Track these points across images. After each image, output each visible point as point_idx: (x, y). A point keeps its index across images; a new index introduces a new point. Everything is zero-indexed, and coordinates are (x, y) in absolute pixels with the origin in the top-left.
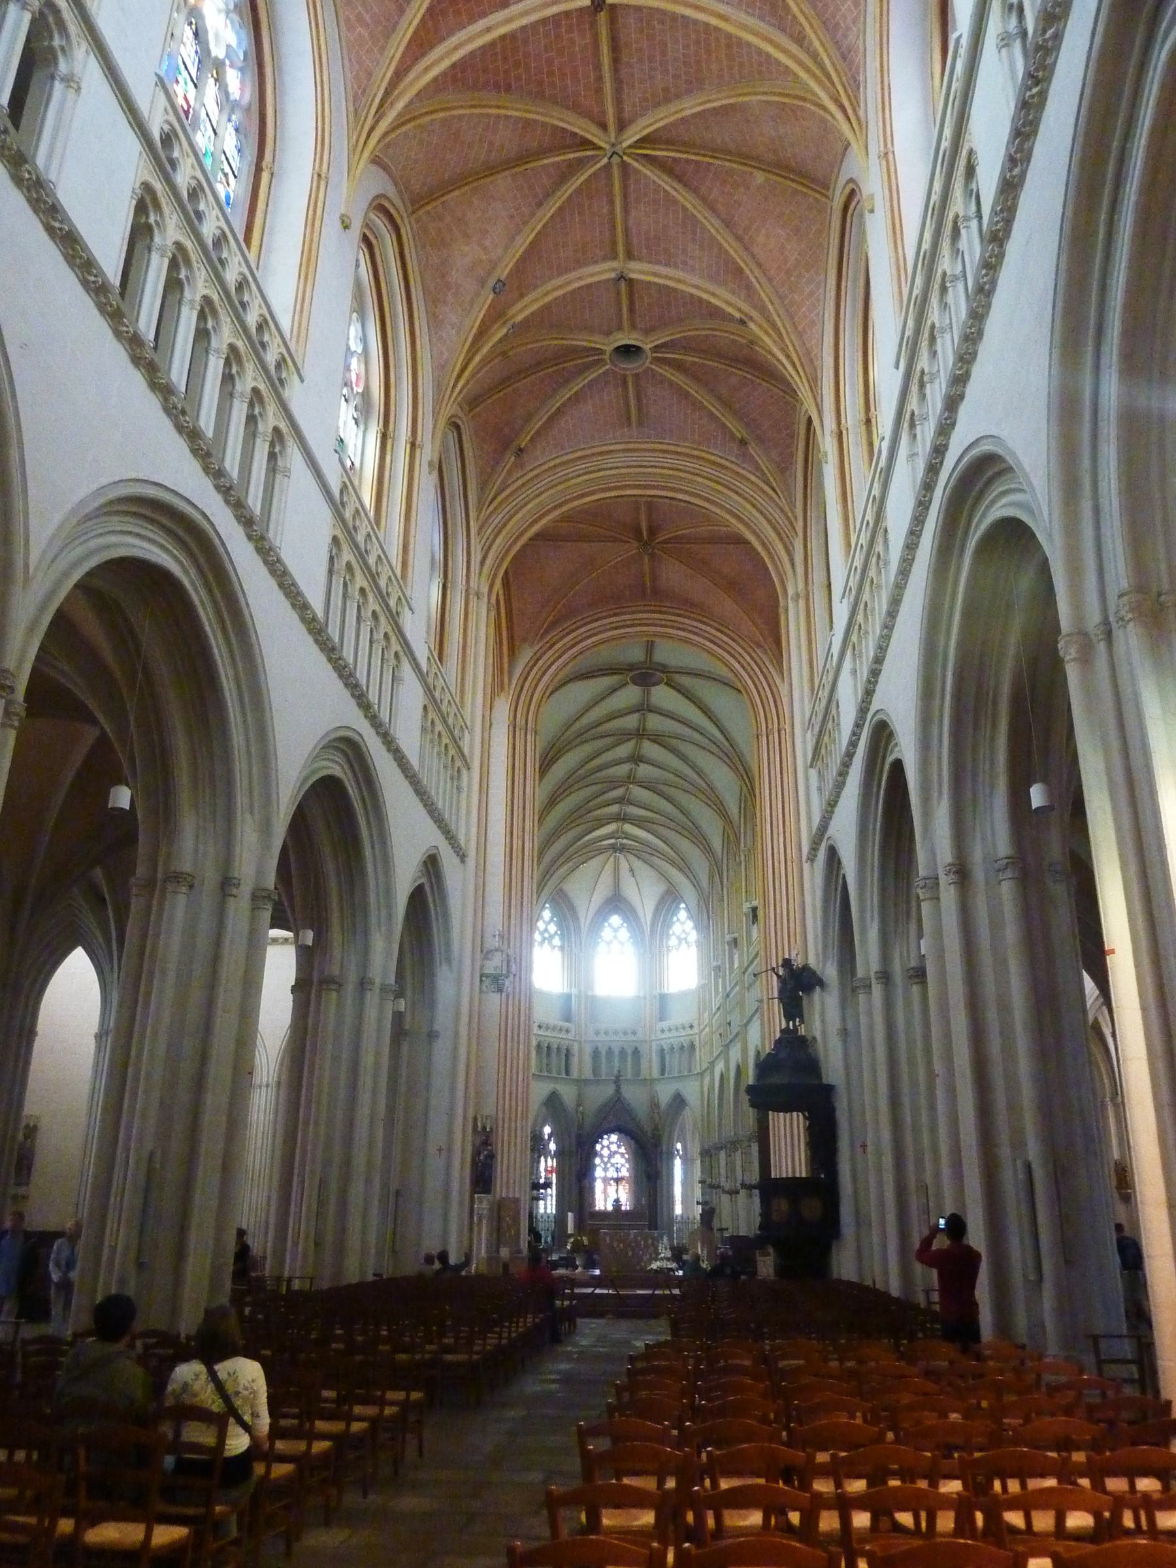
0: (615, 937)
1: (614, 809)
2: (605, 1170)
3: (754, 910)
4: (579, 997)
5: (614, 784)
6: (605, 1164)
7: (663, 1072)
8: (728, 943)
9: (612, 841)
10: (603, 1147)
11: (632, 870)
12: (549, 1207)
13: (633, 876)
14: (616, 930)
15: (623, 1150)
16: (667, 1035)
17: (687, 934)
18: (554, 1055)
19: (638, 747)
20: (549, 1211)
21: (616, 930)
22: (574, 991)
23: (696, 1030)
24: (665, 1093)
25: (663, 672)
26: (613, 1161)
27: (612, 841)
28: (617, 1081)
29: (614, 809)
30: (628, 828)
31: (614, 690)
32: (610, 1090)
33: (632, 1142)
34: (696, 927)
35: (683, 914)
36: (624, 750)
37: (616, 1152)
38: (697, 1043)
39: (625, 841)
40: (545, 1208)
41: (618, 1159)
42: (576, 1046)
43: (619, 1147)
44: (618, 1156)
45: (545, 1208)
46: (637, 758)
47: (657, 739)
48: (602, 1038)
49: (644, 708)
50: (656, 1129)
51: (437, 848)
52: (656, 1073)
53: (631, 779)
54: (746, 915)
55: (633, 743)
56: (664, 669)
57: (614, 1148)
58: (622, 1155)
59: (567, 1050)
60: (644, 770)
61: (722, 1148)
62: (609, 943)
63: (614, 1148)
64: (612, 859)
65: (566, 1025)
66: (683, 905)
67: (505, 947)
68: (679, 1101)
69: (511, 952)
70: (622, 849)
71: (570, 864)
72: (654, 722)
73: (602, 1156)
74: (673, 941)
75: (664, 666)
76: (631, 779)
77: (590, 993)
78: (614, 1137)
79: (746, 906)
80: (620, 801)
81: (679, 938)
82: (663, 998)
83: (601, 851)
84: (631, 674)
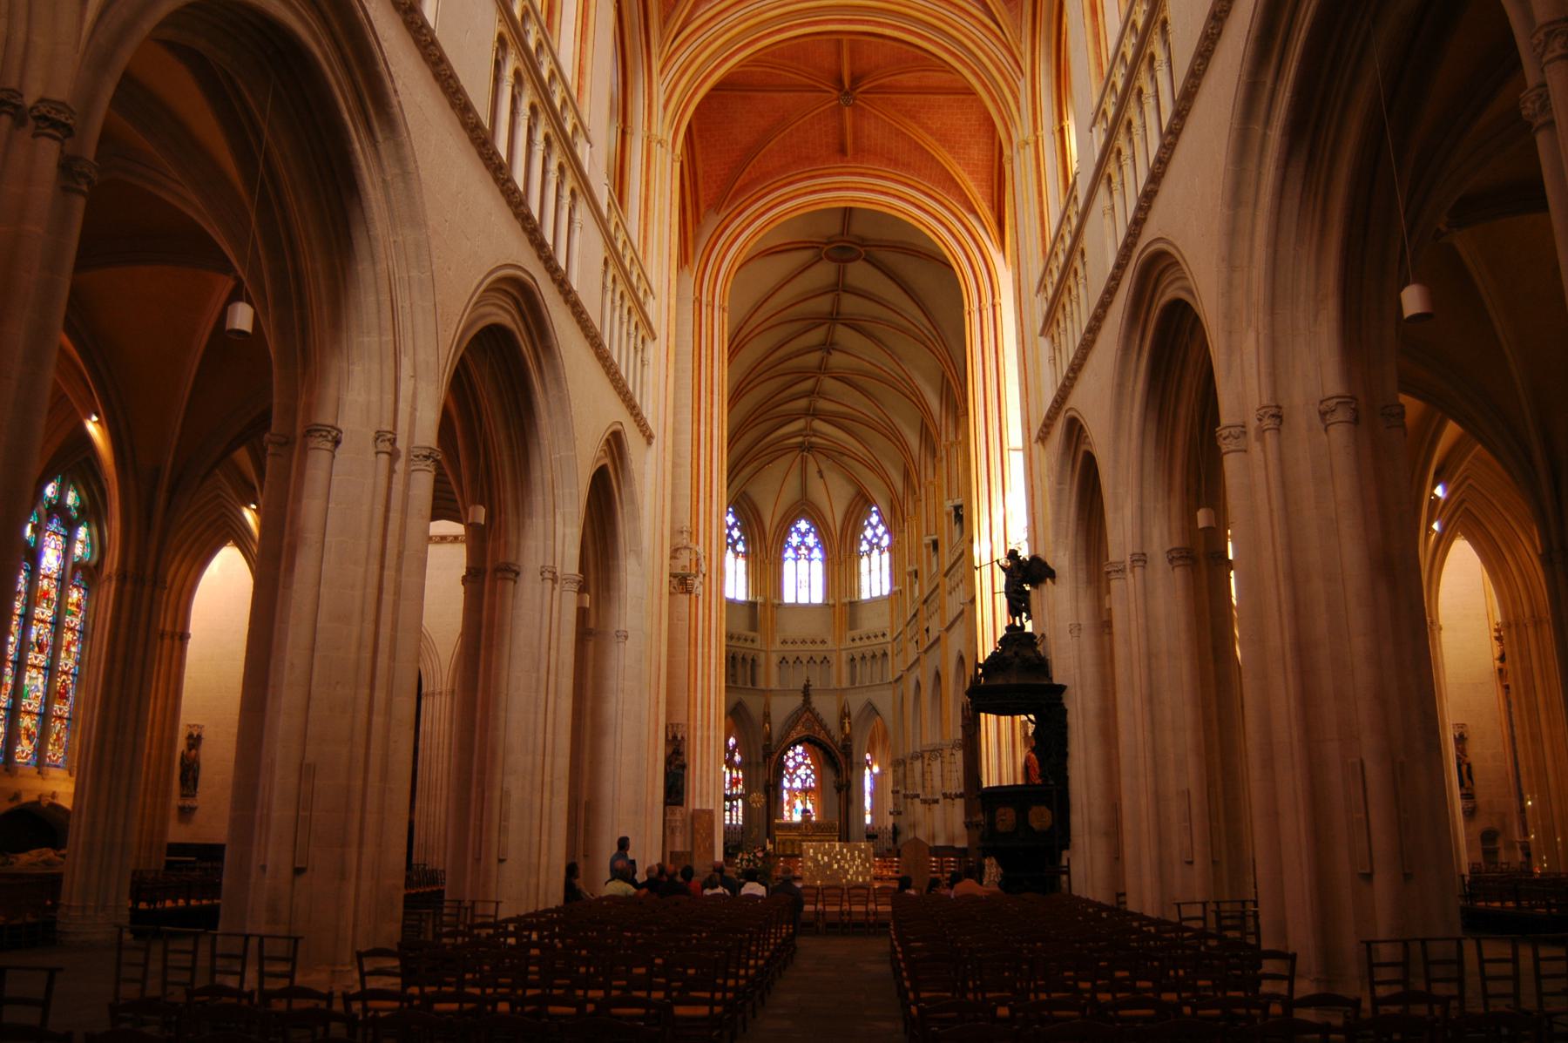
0: (803, 543)
1: (803, 403)
2: (791, 781)
3: (957, 508)
4: (764, 605)
5: (803, 373)
6: (791, 775)
7: (853, 681)
8: (927, 546)
9: (800, 439)
10: (788, 758)
11: (820, 472)
12: (734, 818)
13: (822, 477)
14: (803, 535)
15: (808, 761)
16: (858, 643)
17: (881, 539)
18: (739, 666)
19: (830, 332)
20: (734, 822)
21: (803, 535)
22: (760, 600)
23: (888, 638)
24: (856, 703)
25: (862, 246)
26: (799, 772)
27: (800, 439)
28: (806, 691)
29: (803, 403)
30: (818, 424)
31: (807, 267)
32: (798, 700)
33: (820, 753)
34: (888, 531)
35: (874, 519)
36: (816, 336)
37: (801, 764)
38: (890, 653)
39: (814, 439)
40: (731, 819)
41: (802, 771)
42: (762, 655)
43: (805, 758)
44: (803, 767)
45: (731, 819)
46: (828, 346)
47: (854, 325)
48: (790, 647)
49: (839, 287)
50: (848, 738)
51: (621, 424)
52: (845, 684)
53: (822, 368)
54: (948, 514)
55: (826, 326)
56: (863, 242)
57: (799, 759)
58: (808, 766)
59: (753, 660)
60: (837, 359)
61: (917, 758)
62: (796, 549)
63: (799, 759)
64: (799, 457)
65: (752, 634)
66: (874, 509)
67: (693, 545)
68: (871, 710)
69: (700, 549)
70: (811, 448)
71: (755, 464)
72: (850, 304)
73: (788, 767)
74: (865, 547)
75: (863, 239)
76: (822, 368)
77: (776, 601)
78: (799, 749)
79: (948, 505)
80: (810, 394)
81: (870, 542)
82: (852, 604)
83: (791, 448)
84: (826, 248)
